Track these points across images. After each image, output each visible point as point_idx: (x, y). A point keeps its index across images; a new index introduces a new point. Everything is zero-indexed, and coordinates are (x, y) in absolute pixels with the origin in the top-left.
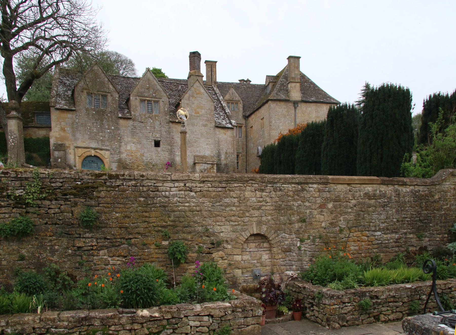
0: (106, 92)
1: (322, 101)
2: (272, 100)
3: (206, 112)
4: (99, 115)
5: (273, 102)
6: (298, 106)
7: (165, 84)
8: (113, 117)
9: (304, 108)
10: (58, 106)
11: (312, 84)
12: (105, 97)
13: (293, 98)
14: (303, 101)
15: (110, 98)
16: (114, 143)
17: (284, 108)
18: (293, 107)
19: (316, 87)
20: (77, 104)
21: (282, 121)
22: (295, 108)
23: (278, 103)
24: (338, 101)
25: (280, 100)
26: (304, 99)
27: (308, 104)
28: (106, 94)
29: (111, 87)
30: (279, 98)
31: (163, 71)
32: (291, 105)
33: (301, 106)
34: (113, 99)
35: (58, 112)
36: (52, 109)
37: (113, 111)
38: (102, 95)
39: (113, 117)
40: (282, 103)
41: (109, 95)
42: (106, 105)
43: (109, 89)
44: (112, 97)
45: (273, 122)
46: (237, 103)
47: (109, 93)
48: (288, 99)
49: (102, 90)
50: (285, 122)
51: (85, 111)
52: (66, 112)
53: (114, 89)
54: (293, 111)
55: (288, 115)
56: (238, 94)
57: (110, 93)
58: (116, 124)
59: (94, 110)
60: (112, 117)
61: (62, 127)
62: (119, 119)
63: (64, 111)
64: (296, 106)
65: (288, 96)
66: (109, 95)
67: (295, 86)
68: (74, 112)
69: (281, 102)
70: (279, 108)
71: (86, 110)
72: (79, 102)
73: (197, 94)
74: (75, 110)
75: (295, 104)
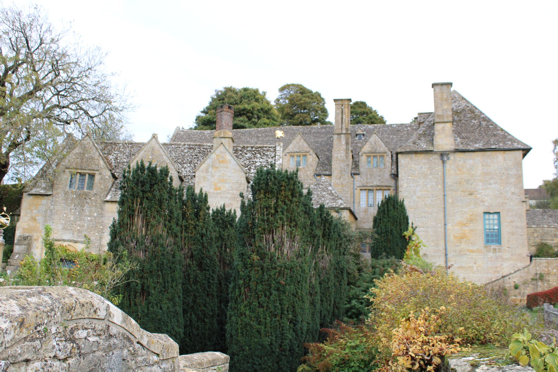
0: (93, 170)
1: (493, 147)
2: (401, 153)
3: (232, 187)
4: (80, 199)
5: (405, 156)
6: (448, 159)
7: (203, 148)
8: (98, 200)
9: (460, 161)
10: (34, 191)
11: (485, 120)
12: (92, 176)
13: (440, 147)
14: (457, 151)
15: (97, 178)
16: (94, 234)
17: (424, 163)
18: (441, 161)
19: (492, 125)
20: (55, 186)
21: (421, 183)
22: (444, 162)
23: (413, 156)
24: (527, 145)
25: (416, 152)
26: (461, 147)
27: (467, 154)
28: (94, 172)
29: (102, 162)
30: (416, 149)
31: (369, 104)
32: (436, 159)
33: (455, 158)
34: (101, 178)
35: (31, 197)
36: (25, 194)
37: (99, 193)
38: (89, 175)
39: (98, 200)
40: (421, 157)
41: (97, 173)
42: (91, 187)
43: (98, 165)
44: (100, 176)
45: (405, 185)
46: (382, 156)
47: (96, 170)
48: (431, 148)
49: (90, 168)
50: (426, 185)
51: (64, 196)
52: (40, 197)
53: (105, 165)
54: (440, 167)
55: (430, 174)
56: (384, 143)
57: (98, 170)
58: (100, 210)
59: (75, 193)
60: (96, 200)
61: (32, 216)
62: (106, 203)
63: (38, 196)
64: (445, 158)
65: (433, 144)
66: (97, 173)
67: (443, 129)
68: (50, 197)
69: (418, 155)
70: (415, 164)
71: (65, 194)
72: (58, 184)
73: (220, 163)
74: (50, 195)
75: (443, 155)
